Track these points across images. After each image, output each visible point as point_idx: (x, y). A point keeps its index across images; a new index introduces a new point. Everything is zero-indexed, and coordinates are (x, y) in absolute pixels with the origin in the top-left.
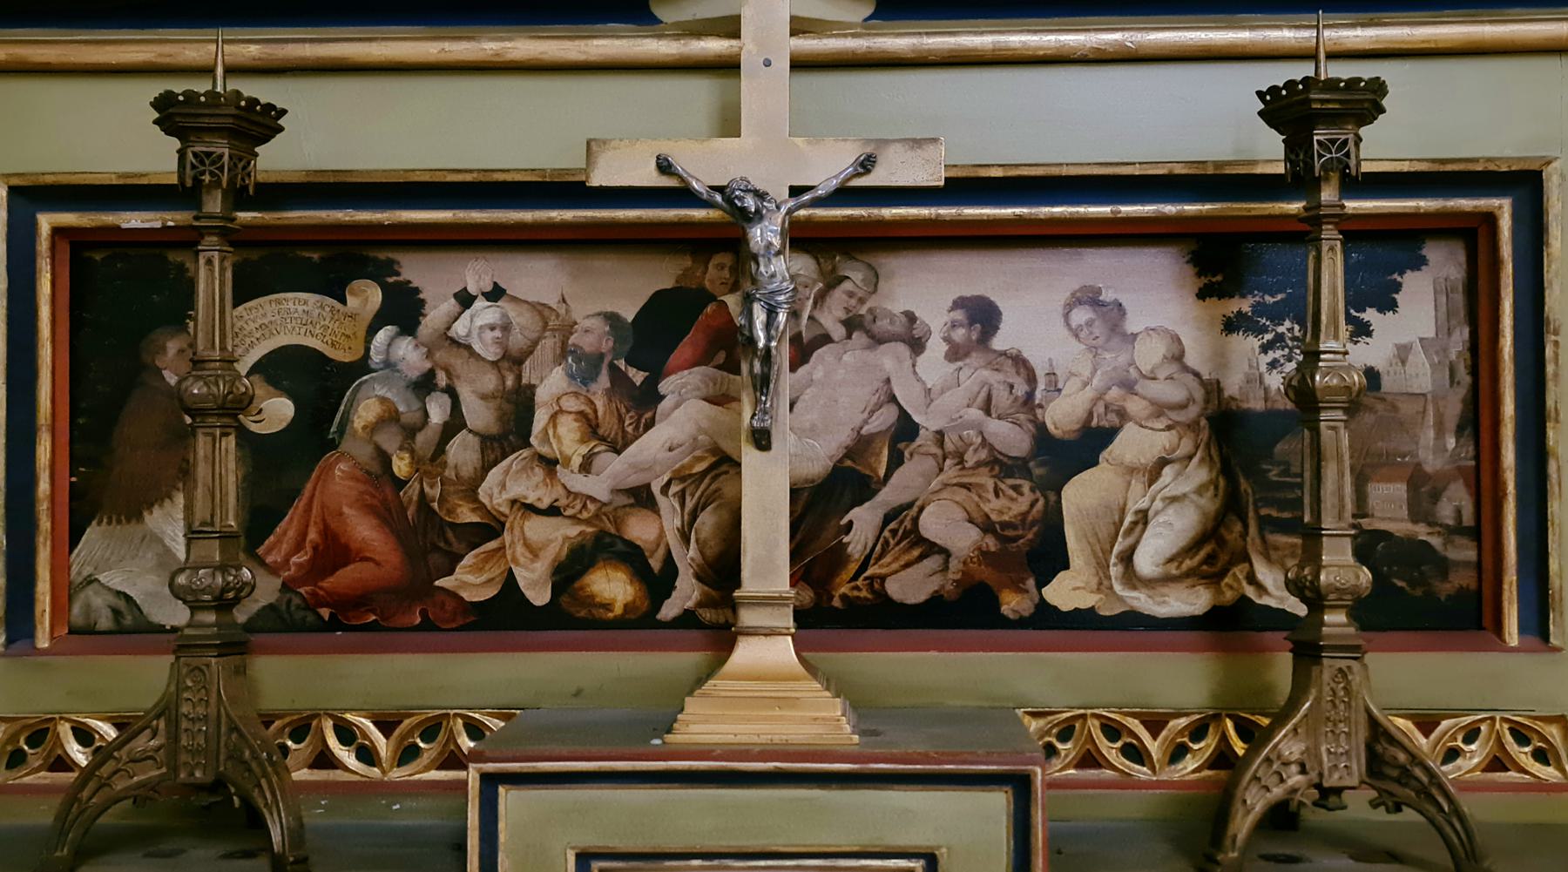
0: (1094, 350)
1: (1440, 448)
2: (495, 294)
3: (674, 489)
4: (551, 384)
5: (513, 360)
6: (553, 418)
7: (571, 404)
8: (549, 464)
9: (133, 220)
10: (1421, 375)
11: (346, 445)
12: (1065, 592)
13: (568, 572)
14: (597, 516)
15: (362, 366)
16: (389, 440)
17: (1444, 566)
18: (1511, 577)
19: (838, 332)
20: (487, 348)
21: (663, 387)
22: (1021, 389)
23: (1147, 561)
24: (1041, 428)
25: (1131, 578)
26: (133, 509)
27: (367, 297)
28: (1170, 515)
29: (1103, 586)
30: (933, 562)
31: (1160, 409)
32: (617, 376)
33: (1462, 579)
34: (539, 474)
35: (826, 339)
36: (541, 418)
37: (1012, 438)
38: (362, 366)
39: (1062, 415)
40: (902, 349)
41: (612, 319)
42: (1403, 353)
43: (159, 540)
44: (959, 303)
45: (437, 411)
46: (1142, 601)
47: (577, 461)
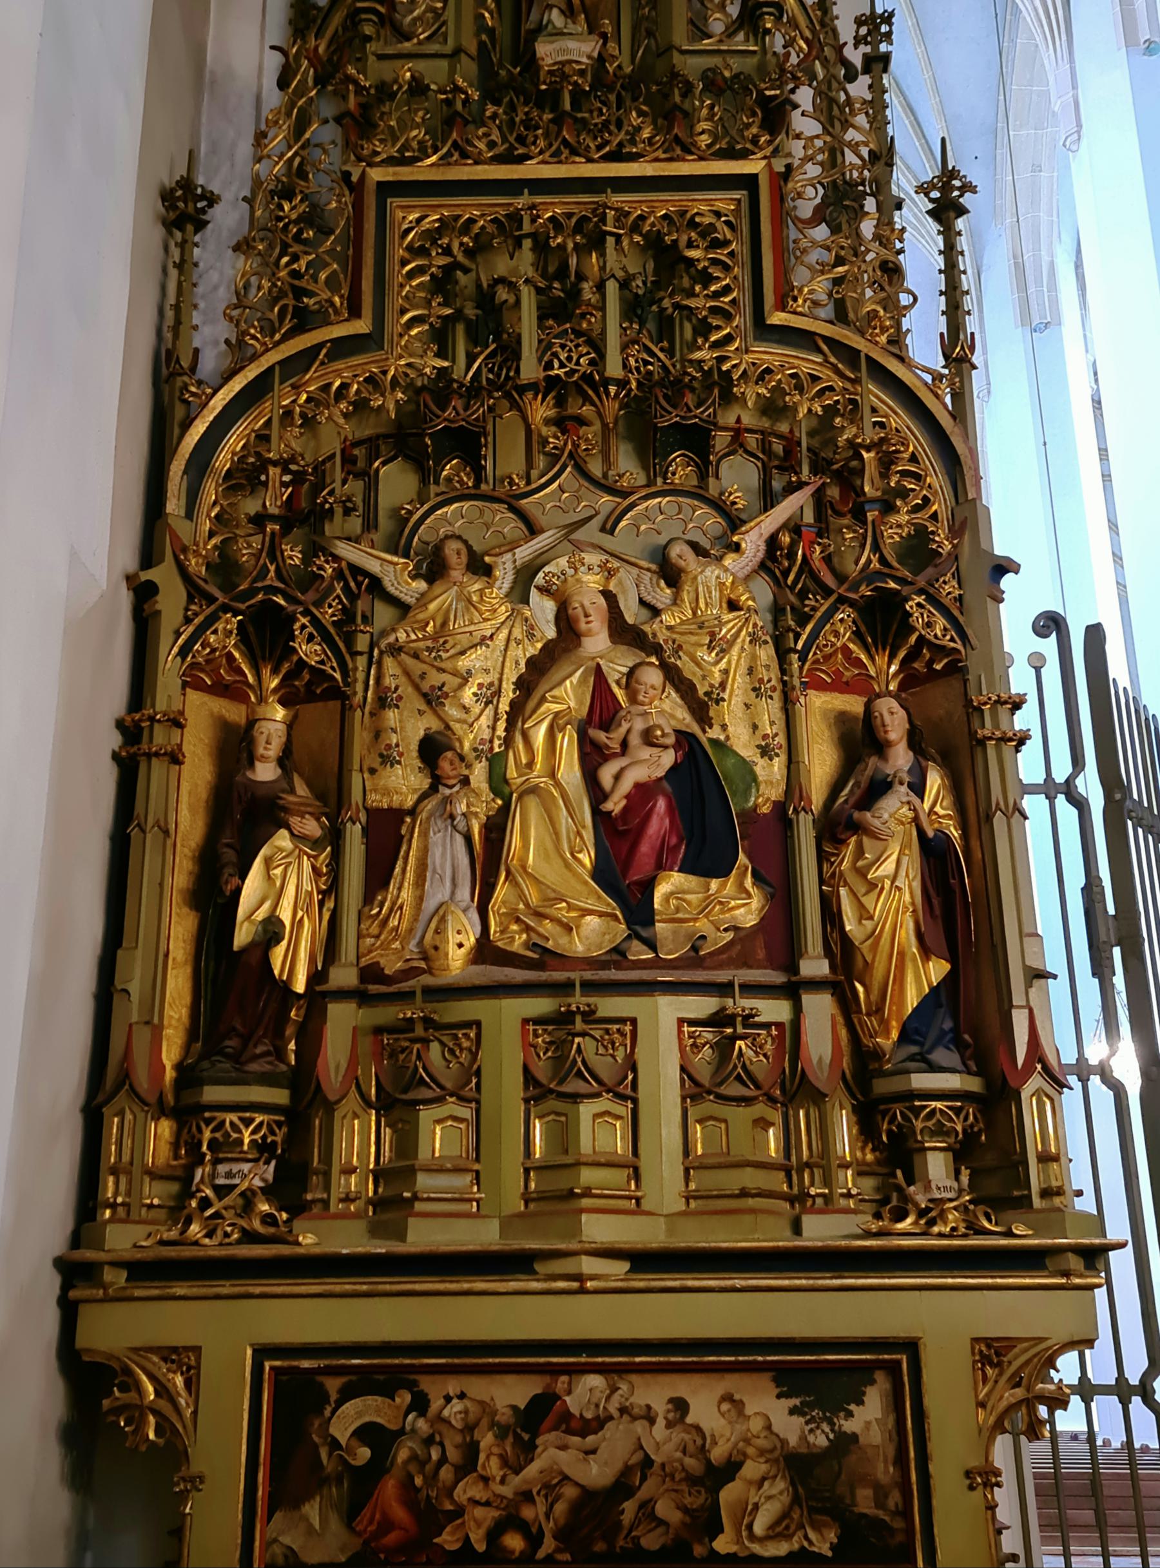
1: (886, 1471)
2: (462, 1396)
3: (543, 1493)
4: (487, 1440)
5: (470, 1428)
6: (488, 1457)
7: (495, 1450)
8: (486, 1480)
9: (306, 1364)
11: (394, 1471)
13: (494, 1535)
14: (507, 1506)
15: (402, 1432)
16: (412, 1468)
17: (891, 1531)
18: (918, 1536)
19: (616, 1414)
20: (457, 1423)
21: (539, 1441)
22: (699, 1442)
23: (759, 1529)
24: (709, 1461)
25: (752, 1537)
26: (296, 1504)
27: (404, 1398)
28: (768, 1506)
29: (739, 1541)
30: (661, 1530)
31: (762, 1452)
32: (517, 1437)
33: (900, 1538)
34: (481, 1485)
35: (611, 1418)
36: (482, 1457)
38: (402, 1432)
39: (717, 1454)
40: (645, 1423)
41: (514, 1408)
42: (868, 1424)
43: (307, 1520)
45: (435, 1455)
46: (756, 1548)
47: (498, 1479)
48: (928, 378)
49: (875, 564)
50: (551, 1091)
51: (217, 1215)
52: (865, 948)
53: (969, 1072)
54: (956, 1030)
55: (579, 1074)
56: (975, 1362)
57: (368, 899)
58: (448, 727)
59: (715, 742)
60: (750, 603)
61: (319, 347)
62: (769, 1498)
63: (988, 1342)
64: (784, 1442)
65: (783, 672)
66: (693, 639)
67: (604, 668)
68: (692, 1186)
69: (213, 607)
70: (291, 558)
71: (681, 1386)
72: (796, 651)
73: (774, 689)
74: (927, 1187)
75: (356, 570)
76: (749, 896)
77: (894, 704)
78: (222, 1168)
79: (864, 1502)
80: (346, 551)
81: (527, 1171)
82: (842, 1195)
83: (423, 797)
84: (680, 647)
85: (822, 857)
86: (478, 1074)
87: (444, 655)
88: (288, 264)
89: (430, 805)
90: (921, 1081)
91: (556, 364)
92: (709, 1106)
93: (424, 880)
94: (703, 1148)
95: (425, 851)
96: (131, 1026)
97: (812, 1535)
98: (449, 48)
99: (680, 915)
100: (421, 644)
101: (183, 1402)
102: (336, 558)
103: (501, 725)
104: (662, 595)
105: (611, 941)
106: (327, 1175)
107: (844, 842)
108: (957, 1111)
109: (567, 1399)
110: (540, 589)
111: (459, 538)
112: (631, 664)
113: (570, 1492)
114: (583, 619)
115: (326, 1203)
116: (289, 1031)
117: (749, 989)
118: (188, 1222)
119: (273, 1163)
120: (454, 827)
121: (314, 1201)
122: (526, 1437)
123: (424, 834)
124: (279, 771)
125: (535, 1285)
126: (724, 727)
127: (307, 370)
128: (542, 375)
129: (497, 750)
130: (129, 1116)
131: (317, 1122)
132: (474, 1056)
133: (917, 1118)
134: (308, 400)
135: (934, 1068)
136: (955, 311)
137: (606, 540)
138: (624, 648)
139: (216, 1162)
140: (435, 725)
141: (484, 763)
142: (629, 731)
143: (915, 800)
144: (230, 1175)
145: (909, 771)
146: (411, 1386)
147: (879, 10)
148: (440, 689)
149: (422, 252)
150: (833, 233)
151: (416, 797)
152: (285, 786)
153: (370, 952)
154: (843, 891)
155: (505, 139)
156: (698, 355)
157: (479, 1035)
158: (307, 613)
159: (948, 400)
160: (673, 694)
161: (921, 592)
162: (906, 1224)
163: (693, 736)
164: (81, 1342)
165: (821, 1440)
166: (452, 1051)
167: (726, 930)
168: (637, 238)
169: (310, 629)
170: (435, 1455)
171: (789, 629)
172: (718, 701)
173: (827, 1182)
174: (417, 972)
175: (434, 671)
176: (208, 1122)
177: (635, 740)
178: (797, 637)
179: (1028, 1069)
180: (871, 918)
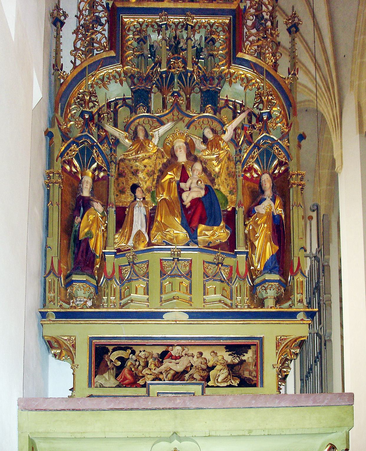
2: (144, 351)
3: (165, 372)
4: (150, 361)
5: (146, 358)
8: (150, 369)
10: (250, 360)
12: (210, 384)
14: (156, 375)
16: (132, 366)
17: (253, 381)
22: (205, 362)
32: (158, 360)
33: (254, 382)
34: (149, 370)
35: (183, 356)
36: (149, 364)
37: (204, 367)
39: (210, 364)
41: (158, 354)
42: (248, 358)
43: (105, 377)
45: (137, 363)
46: (219, 385)
47: (154, 369)
64: (227, 362)
79: (246, 374)
97: (232, 381)
113: (172, 372)
165: (236, 361)
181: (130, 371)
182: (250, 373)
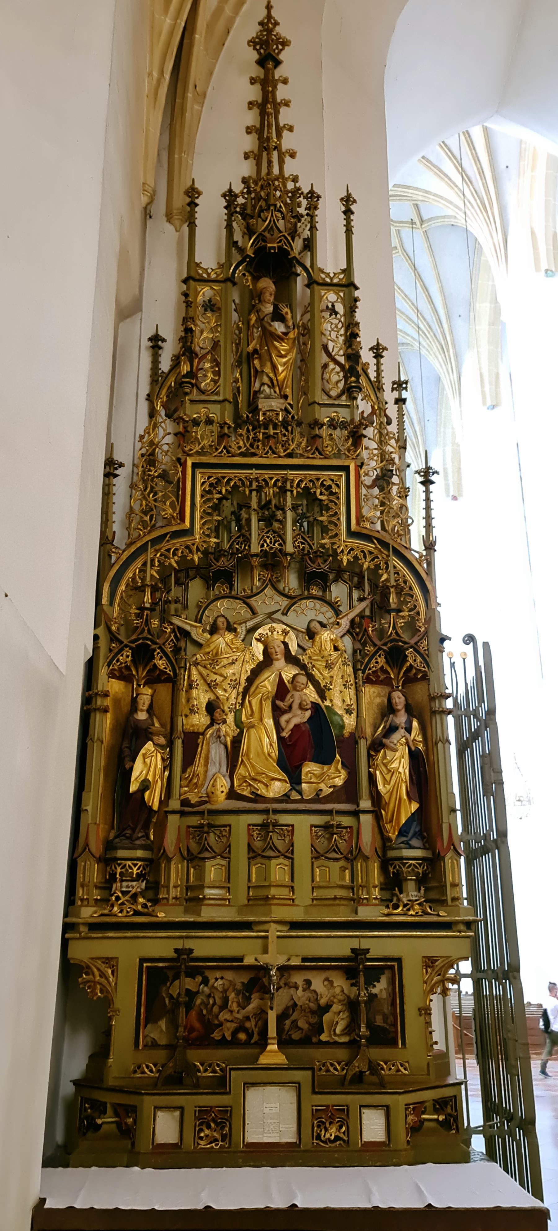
0: (328, 990)
1: (388, 1009)
2: (222, 978)
4: (232, 996)
5: (225, 991)
6: (232, 1003)
7: (235, 1000)
8: (231, 1012)
9: (161, 965)
10: (384, 995)
11: (195, 1008)
12: (324, 1037)
13: (234, 1033)
15: (198, 992)
18: (399, 1034)
19: (283, 986)
20: (220, 989)
21: (253, 996)
22: (316, 997)
23: (338, 1031)
24: (319, 1005)
25: (335, 1034)
27: (199, 979)
29: (330, 1036)
30: (300, 1031)
31: (340, 1001)
34: (229, 1014)
35: (281, 987)
38: (198, 992)
39: (323, 1002)
40: (295, 989)
41: (243, 983)
42: (381, 990)
43: (160, 1027)
44: (305, 980)
45: (211, 1001)
46: (336, 1039)
48: (417, 555)
49: (394, 634)
50: (259, 855)
51: (123, 904)
52: (386, 797)
53: (425, 848)
54: (420, 831)
55: (271, 848)
56: (423, 966)
57: (184, 770)
58: (218, 698)
59: (327, 707)
60: (344, 648)
61: (166, 535)
62: (342, 1019)
63: (429, 958)
65: (356, 678)
66: (319, 663)
67: (282, 674)
68: (315, 894)
69: (122, 645)
70: (154, 624)
71: (309, 975)
72: (360, 670)
73: (352, 685)
74: (408, 895)
75: (179, 628)
76: (340, 773)
77: (400, 695)
78: (124, 884)
80: (176, 621)
81: (249, 888)
82: (374, 898)
83: (208, 727)
84: (314, 666)
85: (369, 756)
86: (229, 846)
87: (217, 668)
88: (153, 496)
89: (210, 732)
90: (406, 853)
91: (265, 545)
92: (322, 861)
93: (208, 764)
94: (320, 879)
95: (208, 751)
96: (88, 825)
98: (221, 398)
99: (312, 780)
100: (207, 662)
101: (111, 980)
102: (172, 624)
103: (240, 697)
104: (307, 644)
105: (284, 791)
106: (168, 887)
107: (379, 751)
108: (420, 865)
109: (264, 980)
110: (256, 639)
111: (223, 616)
112: (294, 673)
114: (274, 654)
115: (167, 899)
116: (152, 826)
117: (340, 813)
118: (112, 906)
119: (145, 882)
120: (220, 741)
121: (163, 898)
122: (247, 994)
123: (208, 744)
124: (148, 715)
125: (252, 934)
126: (331, 701)
127: (162, 542)
128: (260, 549)
129: (238, 708)
130: (88, 863)
131: (163, 865)
132: (228, 839)
133: (404, 867)
134: (161, 555)
135: (412, 847)
136: (429, 527)
137: (284, 619)
138: (291, 665)
139: (122, 881)
140: (213, 697)
141: (233, 713)
142: (293, 702)
143: (407, 735)
144: (127, 887)
145: (405, 723)
146: (202, 974)
147: (402, 379)
148: (215, 681)
149: (209, 492)
150: (380, 492)
151: (204, 727)
152: (150, 721)
153: (185, 793)
154: (378, 772)
155: (245, 446)
156: (324, 541)
157: (230, 830)
158: (160, 648)
159: (425, 566)
160: (311, 687)
161: (411, 647)
162: (399, 910)
163: (318, 705)
164: (70, 955)
166: (219, 837)
167: (330, 787)
168: (299, 489)
169: (161, 654)
170: (211, 1001)
171: (359, 661)
172: (329, 689)
173: (368, 893)
174: (206, 802)
175: (212, 674)
176: (119, 865)
177: (295, 706)
178: (362, 663)
179: (448, 849)
180: (389, 784)
181: (200, 1014)
182: (385, 1018)
